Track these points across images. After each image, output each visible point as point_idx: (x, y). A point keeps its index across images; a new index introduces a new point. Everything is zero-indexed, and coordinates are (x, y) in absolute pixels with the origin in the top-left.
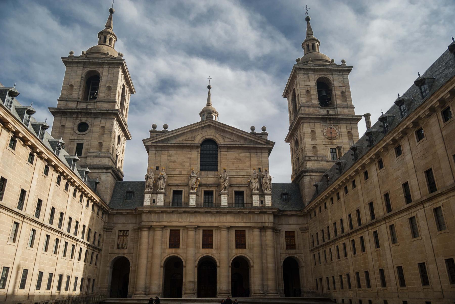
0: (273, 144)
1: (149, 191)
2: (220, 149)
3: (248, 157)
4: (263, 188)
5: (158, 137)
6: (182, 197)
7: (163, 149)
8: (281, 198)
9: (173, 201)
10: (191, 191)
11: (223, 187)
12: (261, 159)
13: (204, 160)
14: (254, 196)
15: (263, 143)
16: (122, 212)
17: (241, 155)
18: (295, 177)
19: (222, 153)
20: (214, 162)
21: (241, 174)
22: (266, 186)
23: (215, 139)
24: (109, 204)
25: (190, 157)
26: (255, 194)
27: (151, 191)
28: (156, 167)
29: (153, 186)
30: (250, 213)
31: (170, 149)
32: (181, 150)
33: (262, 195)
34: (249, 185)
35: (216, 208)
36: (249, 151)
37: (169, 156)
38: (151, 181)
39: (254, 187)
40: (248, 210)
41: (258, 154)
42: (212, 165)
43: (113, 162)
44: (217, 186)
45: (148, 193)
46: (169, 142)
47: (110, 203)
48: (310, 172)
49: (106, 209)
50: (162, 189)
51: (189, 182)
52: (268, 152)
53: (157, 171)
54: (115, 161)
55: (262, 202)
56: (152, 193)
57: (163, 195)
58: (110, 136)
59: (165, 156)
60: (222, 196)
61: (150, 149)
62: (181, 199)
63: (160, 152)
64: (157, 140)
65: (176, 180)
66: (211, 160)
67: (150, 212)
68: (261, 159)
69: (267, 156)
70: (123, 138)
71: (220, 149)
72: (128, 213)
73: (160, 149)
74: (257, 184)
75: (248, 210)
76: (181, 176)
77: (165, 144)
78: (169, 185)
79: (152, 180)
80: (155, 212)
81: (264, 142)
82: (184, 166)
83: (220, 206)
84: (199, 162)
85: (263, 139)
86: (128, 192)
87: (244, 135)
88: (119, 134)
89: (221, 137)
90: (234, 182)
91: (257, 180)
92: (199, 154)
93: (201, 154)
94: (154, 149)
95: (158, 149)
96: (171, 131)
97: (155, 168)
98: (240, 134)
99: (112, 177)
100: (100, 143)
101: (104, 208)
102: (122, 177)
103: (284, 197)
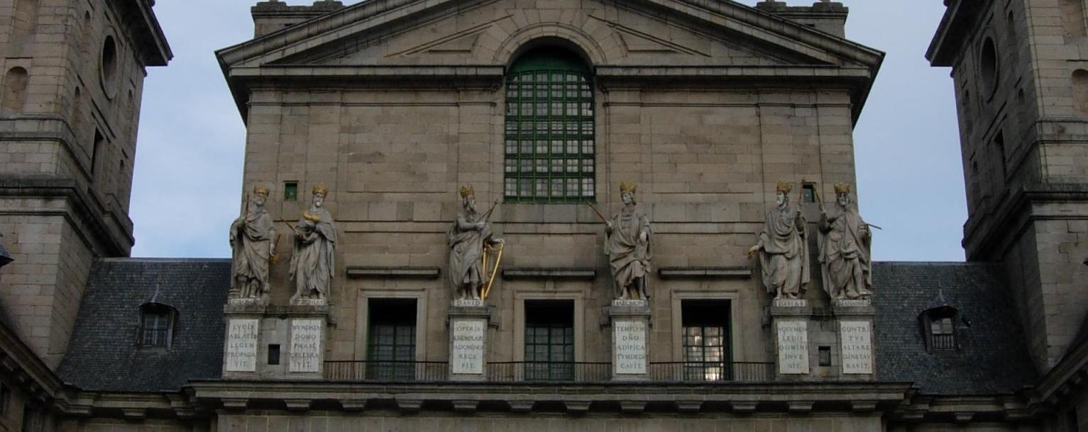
0: (875, 60)
1: (248, 306)
2: (605, 92)
3: (746, 130)
4: (828, 286)
5: (289, 37)
6: (413, 335)
7: (316, 98)
8: (923, 333)
9: (371, 347)
10: (462, 302)
11: (622, 279)
12: (813, 141)
13: (526, 148)
14: (781, 325)
15: (823, 57)
16: (120, 404)
17: (709, 119)
18: (983, 233)
19: (614, 109)
20: (572, 156)
21: (716, 214)
22: (847, 272)
23: (579, 41)
24: (59, 369)
25: (453, 131)
26: (788, 315)
27: (262, 300)
28: (281, 188)
29: (272, 276)
30: (765, 408)
31: (350, 98)
32: (409, 98)
33: (825, 314)
34: (754, 270)
35: (587, 386)
36: (754, 99)
37: (346, 129)
38: (258, 253)
39: (779, 279)
40: (751, 397)
41: (799, 111)
42: (565, 175)
43: (77, 163)
44: (590, 279)
45: (249, 312)
46: (345, 61)
47: (64, 362)
48: (1062, 200)
49: (40, 390)
50: (315, 292)
51: (448, 256)
52: (847, 100)
53: (289, 206)
54: (87, 163)
55: (825, 353)
56: (267, 314)
57: (318, 323)
58: (61, 38)
59: (331, 127)
60: (619, 325)
61: (255, 98)
62: (413, 346)
63: (304, 110)
64: (290, 51)
65: (384, 249)
66: (557, 147)
67: (257, 406)
68: (813, 141)
69: (846, 121)
70: (124, 55)
71: (605, 92)
72: (151, 414)
73: (305, 98)
74: (796, 264)
75: (751, 397)
76: (409, 226)
77: (330, 72)
78: (354, 276)
79: (262, 249)
80: (279, 406)
81: (828, 51)
82: (424, 177)
83: (610, 376)
84: (500, 159)
85: (822, 36)
86: (149, 309)
87: (726, 16)
88: (111, 32)
89: (609, 31)
90: (679, 255)
91: (795, 244)
92: (501, 120)
93: (507, 119)
94: (271, 97)
95: (291, 98)
96: (355, 8)
97: (272, 190)
98: (705, 16)
99: (75, 241)
100: (19, 71)
101: (30, 381)
102: (124, 243)
103: (935, 328)
